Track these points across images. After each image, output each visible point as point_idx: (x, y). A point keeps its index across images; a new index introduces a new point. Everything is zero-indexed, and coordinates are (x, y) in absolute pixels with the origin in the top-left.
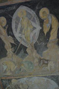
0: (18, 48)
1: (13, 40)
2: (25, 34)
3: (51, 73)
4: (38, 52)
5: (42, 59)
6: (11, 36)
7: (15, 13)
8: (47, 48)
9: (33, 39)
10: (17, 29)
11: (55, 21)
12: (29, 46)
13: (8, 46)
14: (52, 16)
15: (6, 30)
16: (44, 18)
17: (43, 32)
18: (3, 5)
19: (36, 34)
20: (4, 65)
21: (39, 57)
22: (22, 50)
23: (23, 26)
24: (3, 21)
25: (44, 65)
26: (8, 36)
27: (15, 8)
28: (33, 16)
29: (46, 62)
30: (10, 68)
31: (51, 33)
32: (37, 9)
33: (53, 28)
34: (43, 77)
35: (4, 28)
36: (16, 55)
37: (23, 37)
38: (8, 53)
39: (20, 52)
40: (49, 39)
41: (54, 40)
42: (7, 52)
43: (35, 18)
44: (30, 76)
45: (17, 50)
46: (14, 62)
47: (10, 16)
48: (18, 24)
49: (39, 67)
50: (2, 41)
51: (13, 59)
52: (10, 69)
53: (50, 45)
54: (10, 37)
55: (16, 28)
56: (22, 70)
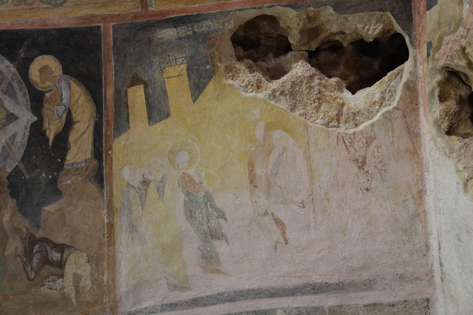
8: (58, 193)
11: (83, 98)
14: (71, 82)
16: (45, 85)
17: (43, 135)
19: (18, 139)
21: (24, 230)
25: (48, 269)
28: (9, 76)
29: (56, 256)
31: (72, 138)
32: (22, 58)
33: (77, 122)
40: (63, 159)
41: (83, 165)
43: (15, 84)
49: (28, 276)
53: (69, 182)
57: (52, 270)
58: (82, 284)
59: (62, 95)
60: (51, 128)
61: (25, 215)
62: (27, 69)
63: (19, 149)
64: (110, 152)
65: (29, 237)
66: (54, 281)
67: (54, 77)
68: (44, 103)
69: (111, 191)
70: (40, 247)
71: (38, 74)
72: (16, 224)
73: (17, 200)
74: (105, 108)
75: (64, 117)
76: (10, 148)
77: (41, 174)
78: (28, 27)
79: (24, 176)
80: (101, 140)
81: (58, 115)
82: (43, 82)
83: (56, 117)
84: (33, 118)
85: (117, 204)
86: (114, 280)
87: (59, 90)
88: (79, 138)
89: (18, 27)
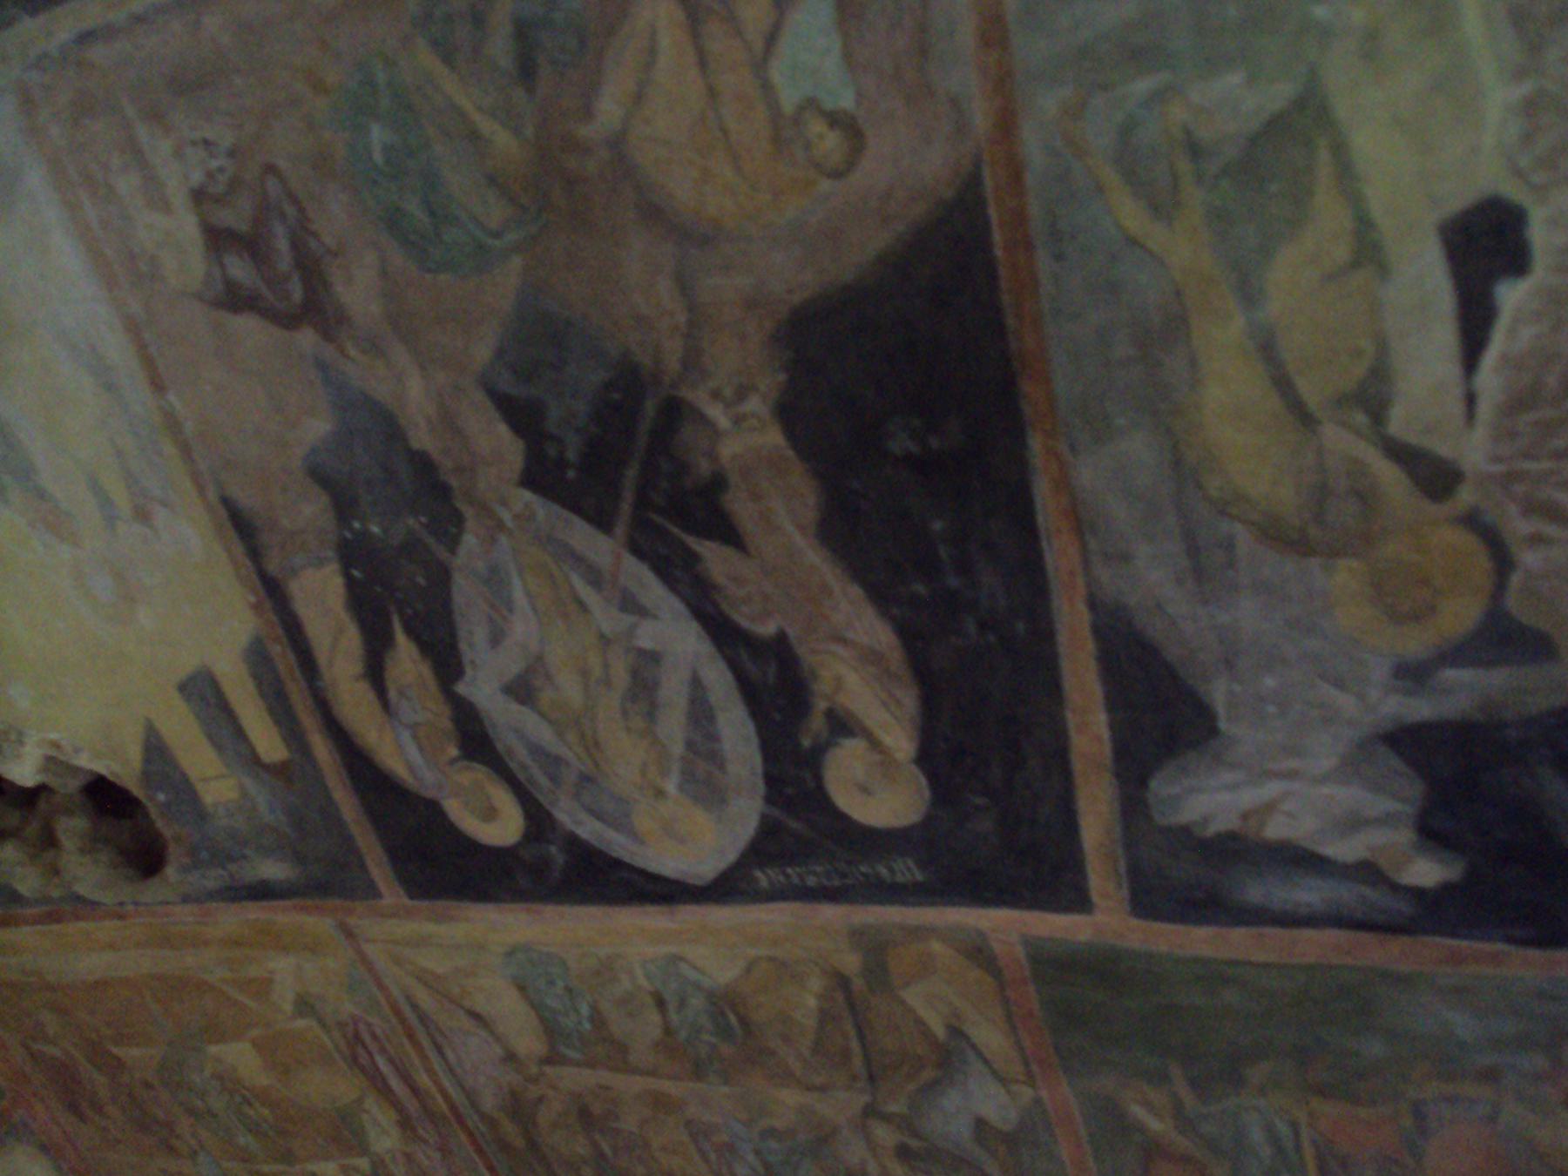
0: (631, 473)
1: (715, 587)
3: (98, 53)
4: (390, 428)
9: (494, 580)
12: (504, 503)
15: (821, 705)
20: (835, 119)
22: (571, 455)
30: (703, 63)
35: (842, 725)
37: (607, 618)
38: (771, 381)
42: (788, 413)
43: (543, 781)
45: (642, 441)
46: (654, 213)
48: (690, 745)
50: (858, 571)
51: (684, 285)
55: (701, 713)
56: (500, 48)
75: (393, 695)
76: (492, 606)
79: (420, 523)
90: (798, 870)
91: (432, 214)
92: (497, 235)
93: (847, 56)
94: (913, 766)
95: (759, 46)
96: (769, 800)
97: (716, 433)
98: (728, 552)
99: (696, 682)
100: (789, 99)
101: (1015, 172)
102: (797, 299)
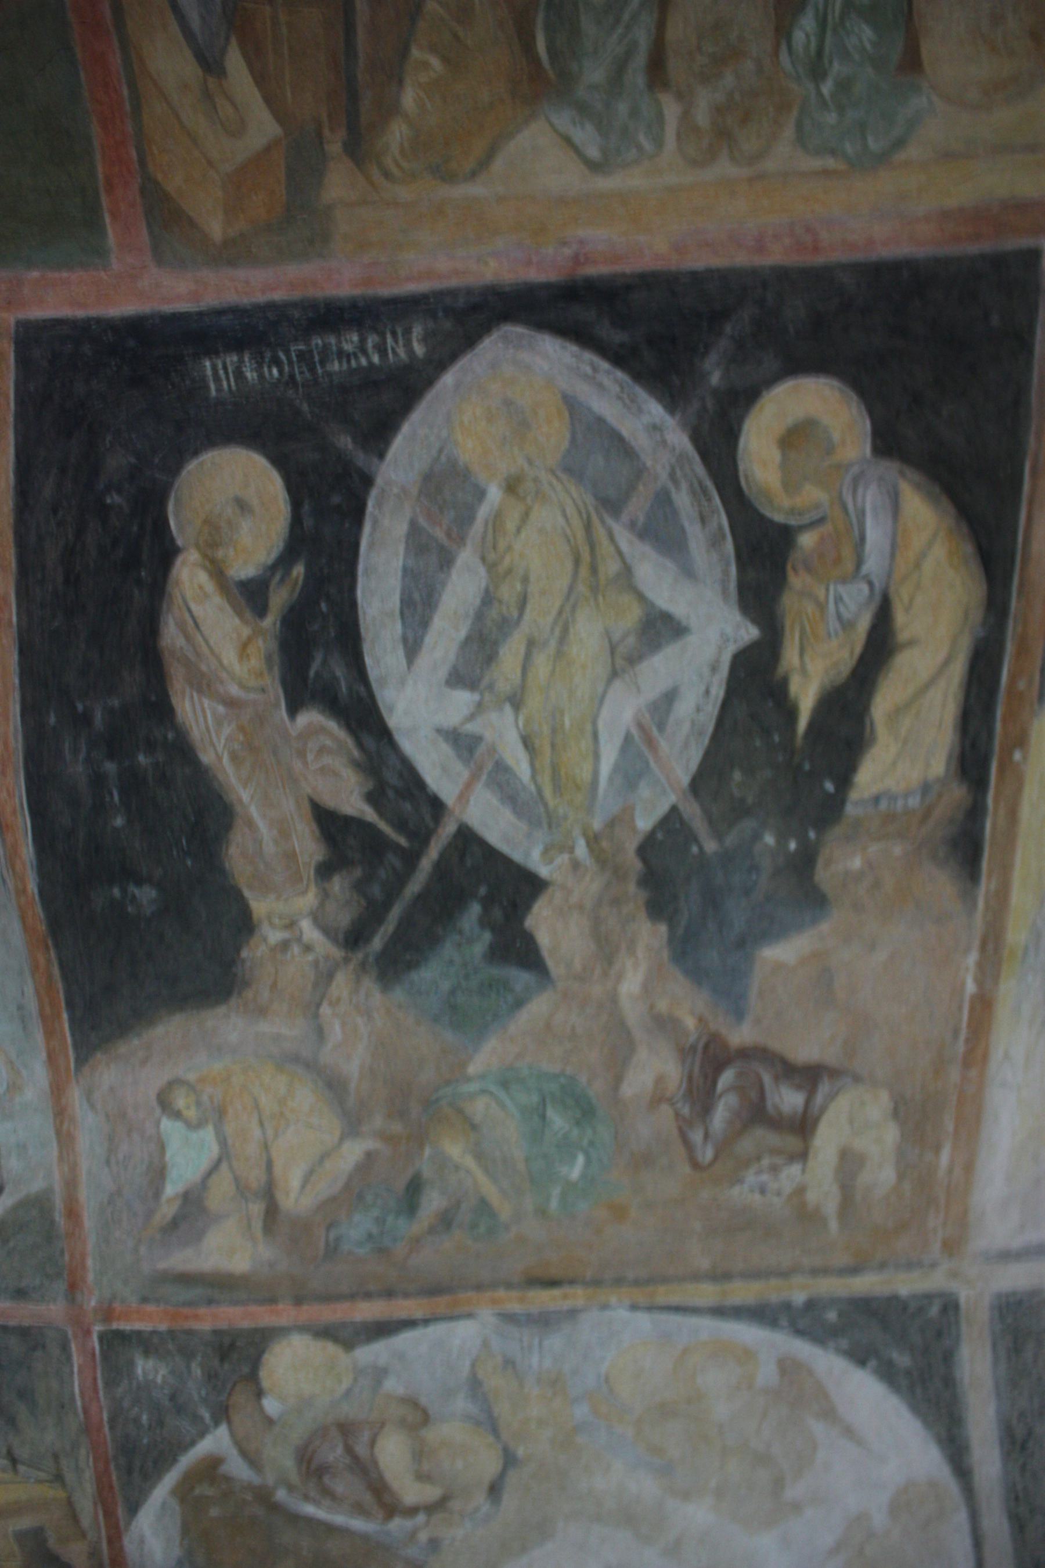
0: (414, 886)
1: (356, 765)
2: (534, 702)
5: (745, 1054)
6: (334, 706)
7: (416, 416)
10: (425, 624)
11: (939, 552)
12: (576, 865)
13: (269, 848)
15: (270, 621)
18: (261, 298)
19: (684, 708)
20: (177, 1115)
21: (690, 1023)
23: (508, 593)
24: (242, 505)
25: (761, 1136)
26: (293, 710)
27: (419, 350)
30: (269, 1165)
33: (911, 643)
34: (737, 1313)
36: (369, 983)
39: (434, 941)
40: (845, 780)
43: (683, 500)
44: (544, 1299)
45: (395, 913)
47: (345, 442)
48: (446, 561)
51: (320, 1033)
52: (255, 1177)
53: (857, 863)
54: (322, 730)
56: (433, 1202)
57: (773, 1139)
58: (864, 1178)
59: (862, 539)
60: (810, 667)
61: (697, 975)
62: (731, 434)
63: (686, 745)
64: (1017, 756)
65: (706, 1046)
66: (774, 1169)
67: (839, 467)
68: (789, 567)
69: (1002, 896)
70: (740, 1075)
71: (776, 455)
72: (662, 1006)
73: (672, 929)
74: (1021, 585)
76: (650, 742)
77: (757, 836)
78: (742, 259)
80: (989, 708)
81: (839, 616)
82: (790, 486)
83: (833, 624)
84: (743, 632)
85: (1016, 935)
86: (969, 1168)
87: (854, 520)
88: (908, 705)
89: (699, 261)
90: (364, 362)
91: (543, 1117)
92: (484, 1091)
93: (162, 1147)
94: (179, 542)
95: (224, 1166)
96: (368, 481)
97: (317, 918)
98: (329, 801)
99: (412, 649)
100: (208, 1134)
101: (51, 1059)
102: (222, 1010)
